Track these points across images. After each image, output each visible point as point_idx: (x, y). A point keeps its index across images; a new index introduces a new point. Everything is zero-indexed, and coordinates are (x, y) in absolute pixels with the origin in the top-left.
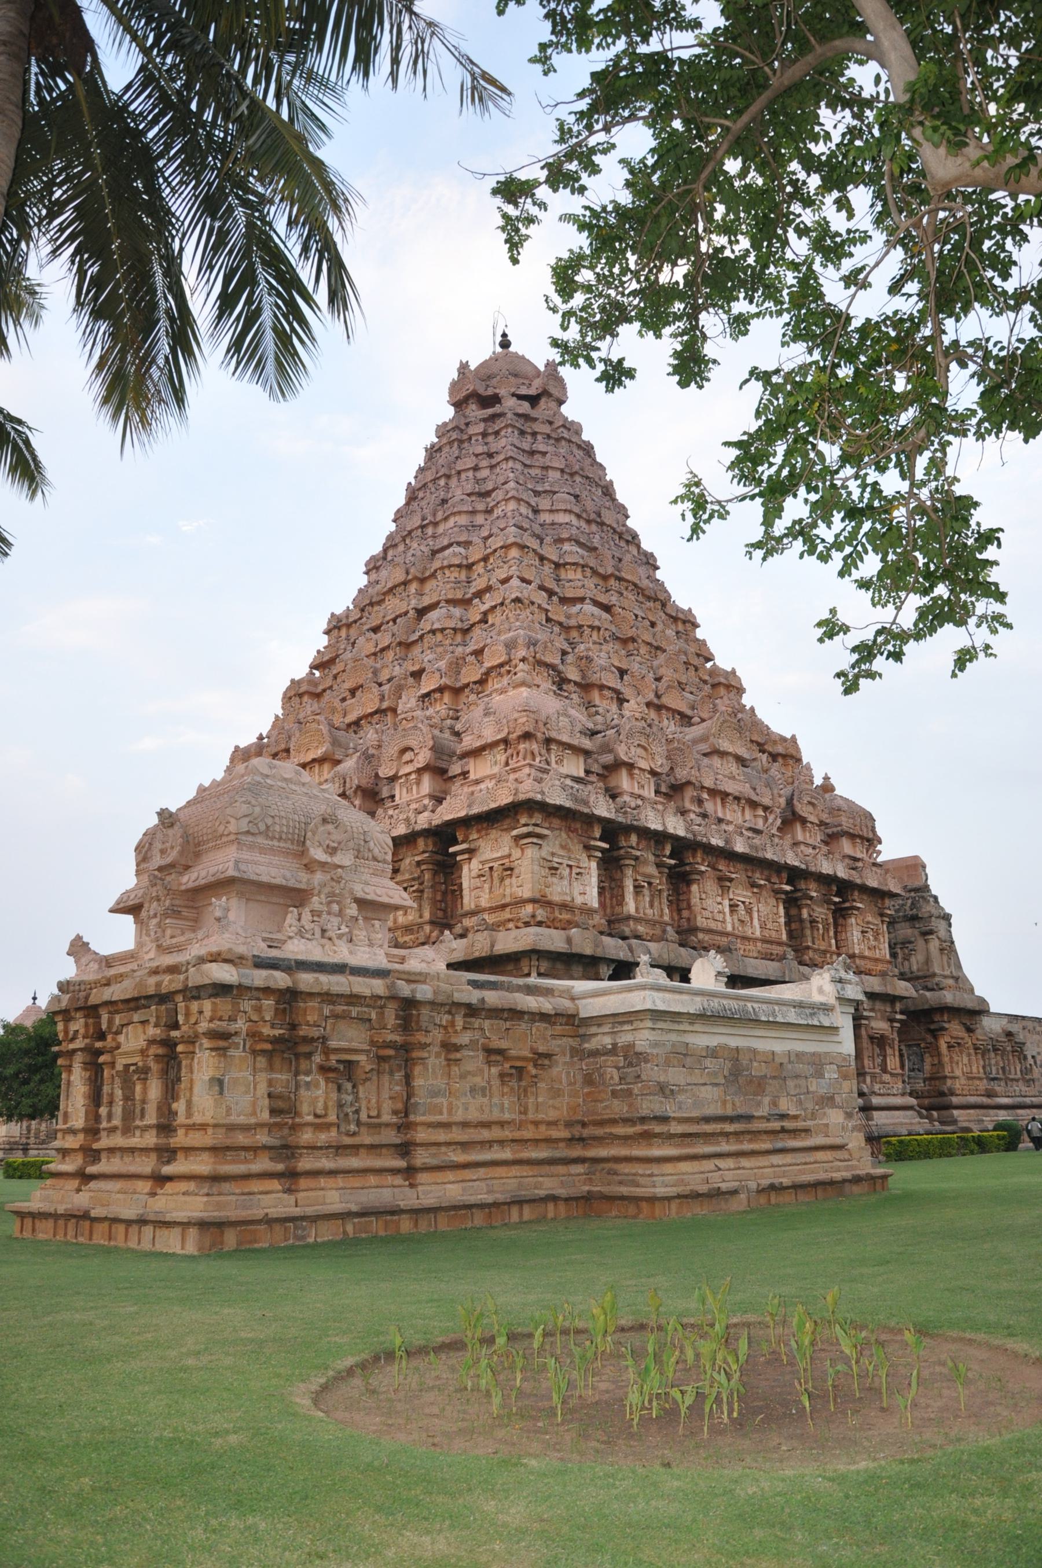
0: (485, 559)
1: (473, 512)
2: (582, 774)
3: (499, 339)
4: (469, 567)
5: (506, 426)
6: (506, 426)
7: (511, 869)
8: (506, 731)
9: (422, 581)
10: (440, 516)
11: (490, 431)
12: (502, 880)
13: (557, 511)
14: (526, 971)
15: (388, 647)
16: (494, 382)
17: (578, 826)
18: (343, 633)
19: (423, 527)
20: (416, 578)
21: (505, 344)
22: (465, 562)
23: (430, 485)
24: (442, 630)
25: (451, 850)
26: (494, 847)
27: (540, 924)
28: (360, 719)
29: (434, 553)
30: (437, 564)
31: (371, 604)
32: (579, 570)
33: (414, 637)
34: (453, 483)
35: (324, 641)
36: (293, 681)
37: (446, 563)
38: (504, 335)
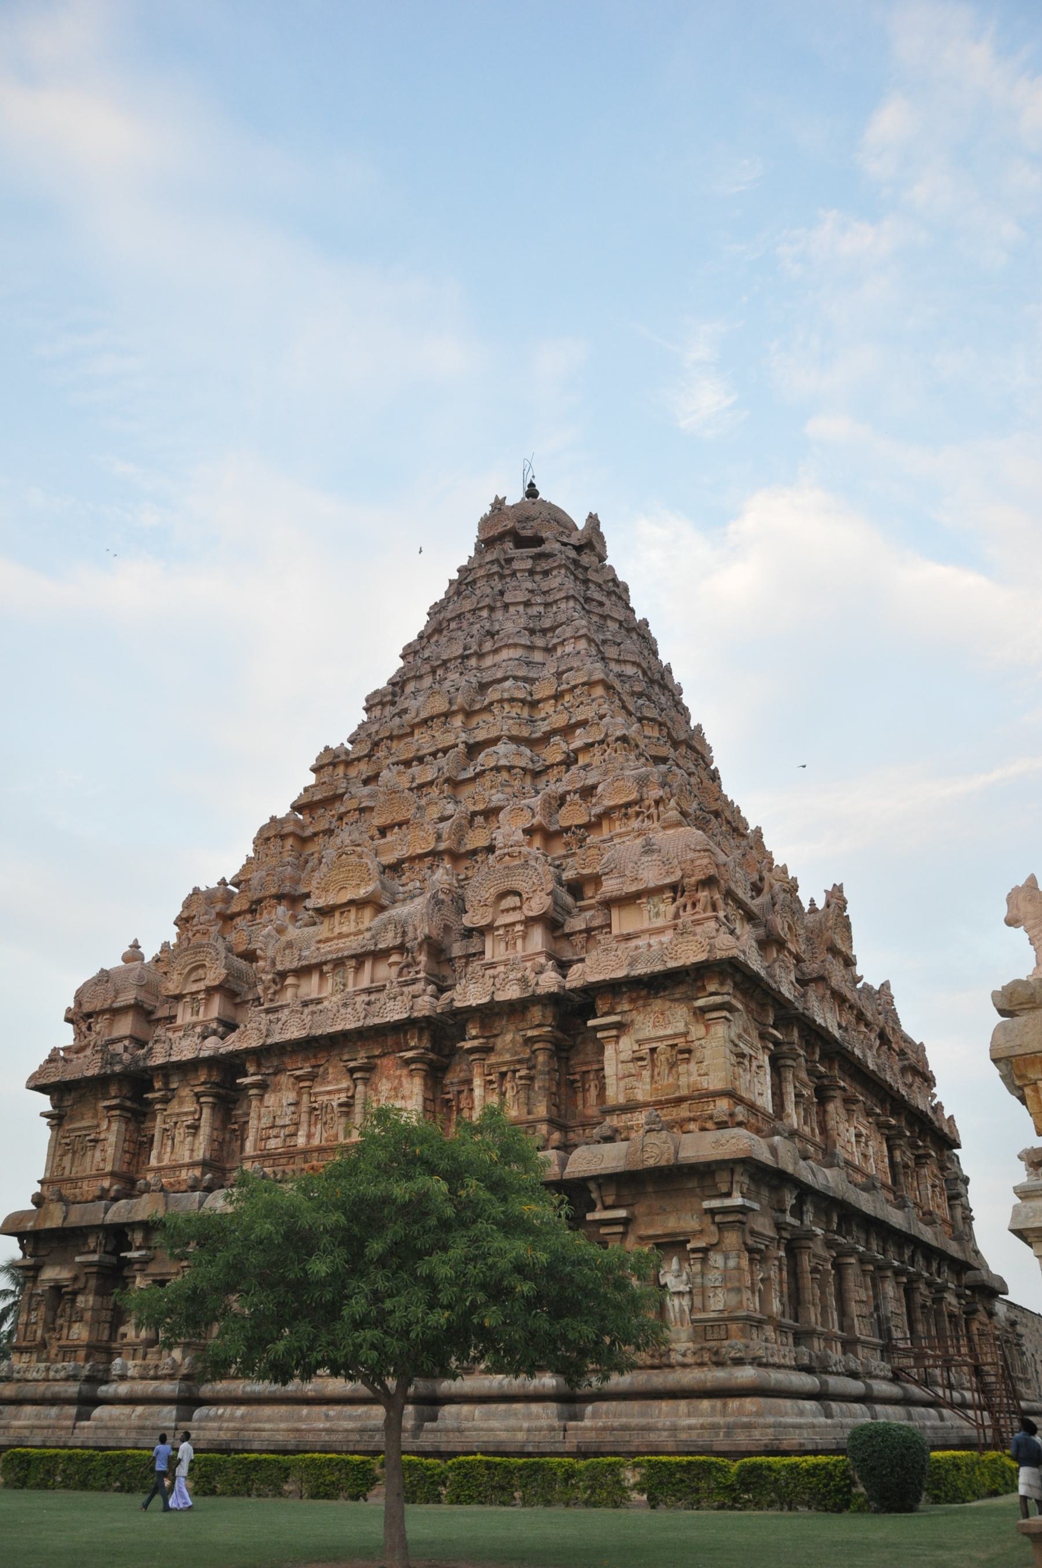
0: (557, 697)
1: (531, 648)
4: (534, 705)
5: (560, 567)
6: (560, 567)
7: (689, 1051)
8: (679, 873)
9: (469, 714)
10: (488, 646)
11: (538, 569)
12: (672, 1065)
13: (625, 662)
14: (724, 1189)
15: (431, 783)
16: (534, 524)
17: (754, 1007)
18: (340, 770)
19: (465, 657)
20: (462, 710)
21: (532, 492)
22: (529, 698)
23: (468, 616)
24: (509, 769)
25: (591, 1023)
26: (660, 1023)
27: (740, 1124)
30: (492, 695)
31: (391, 738)
32: (657, 728)
33: (470, 773)
34: (499, 615)
36: (273, 819)
37: (506, 695)
38: (532, 485)
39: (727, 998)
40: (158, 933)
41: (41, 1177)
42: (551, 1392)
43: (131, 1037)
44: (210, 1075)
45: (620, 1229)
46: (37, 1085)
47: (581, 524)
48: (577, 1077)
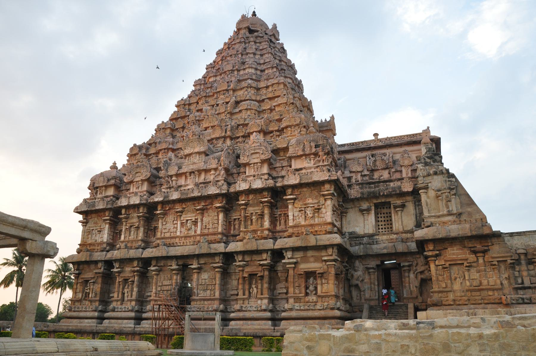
19: (232, 71)
21: (254, 14)
25: (284, 197)
27: (335, 233)
28: (212, 139)
29: (239, 81)
30: (244, 84)
35: (176, 109)
38: (254, 12)
39: (332, 192)
40: (122, 161)
41: (80, 243)
42: (270, 317)
43: (113, 196)
44: (143, 210)
45: (293, 266)
46: (77, 211)
47: (270, 27)
48: (277, 216)
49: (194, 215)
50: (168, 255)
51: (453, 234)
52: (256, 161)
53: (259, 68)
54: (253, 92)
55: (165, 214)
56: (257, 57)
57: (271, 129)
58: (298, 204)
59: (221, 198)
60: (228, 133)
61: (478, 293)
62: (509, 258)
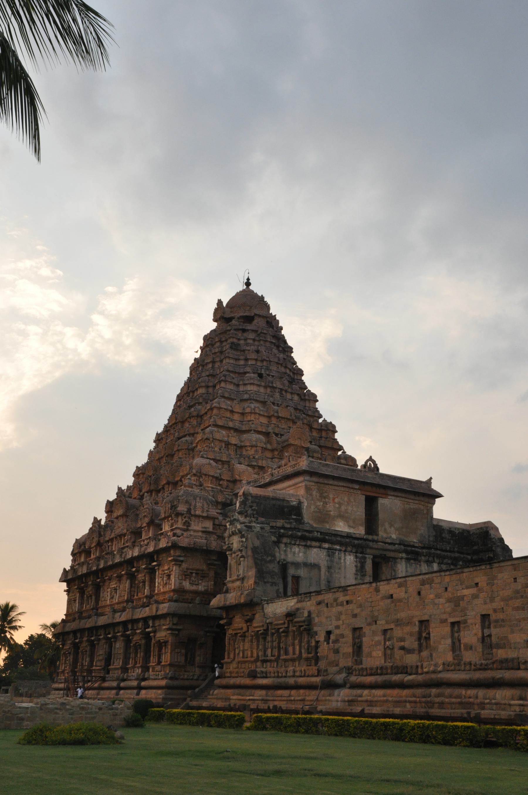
2: (211, 529)
3: (246, 281)
4: (201, 417)
20: (179, 421)
21: (248, 284)
38: (248, 279)
41: (65, 613)
46: (61, 580)
49: (114, 583)
50: (97, 625)
51: (228, 603)
52: (145, 525)
53: (211, 384)
54: (194, 422)
55: (104, 581)
56: (217, 365)
57: (177, 479)
58: (161, 569)
59: (125, 566)
60: (152, 488)
61: (243, 666)
62: (262, 629)
